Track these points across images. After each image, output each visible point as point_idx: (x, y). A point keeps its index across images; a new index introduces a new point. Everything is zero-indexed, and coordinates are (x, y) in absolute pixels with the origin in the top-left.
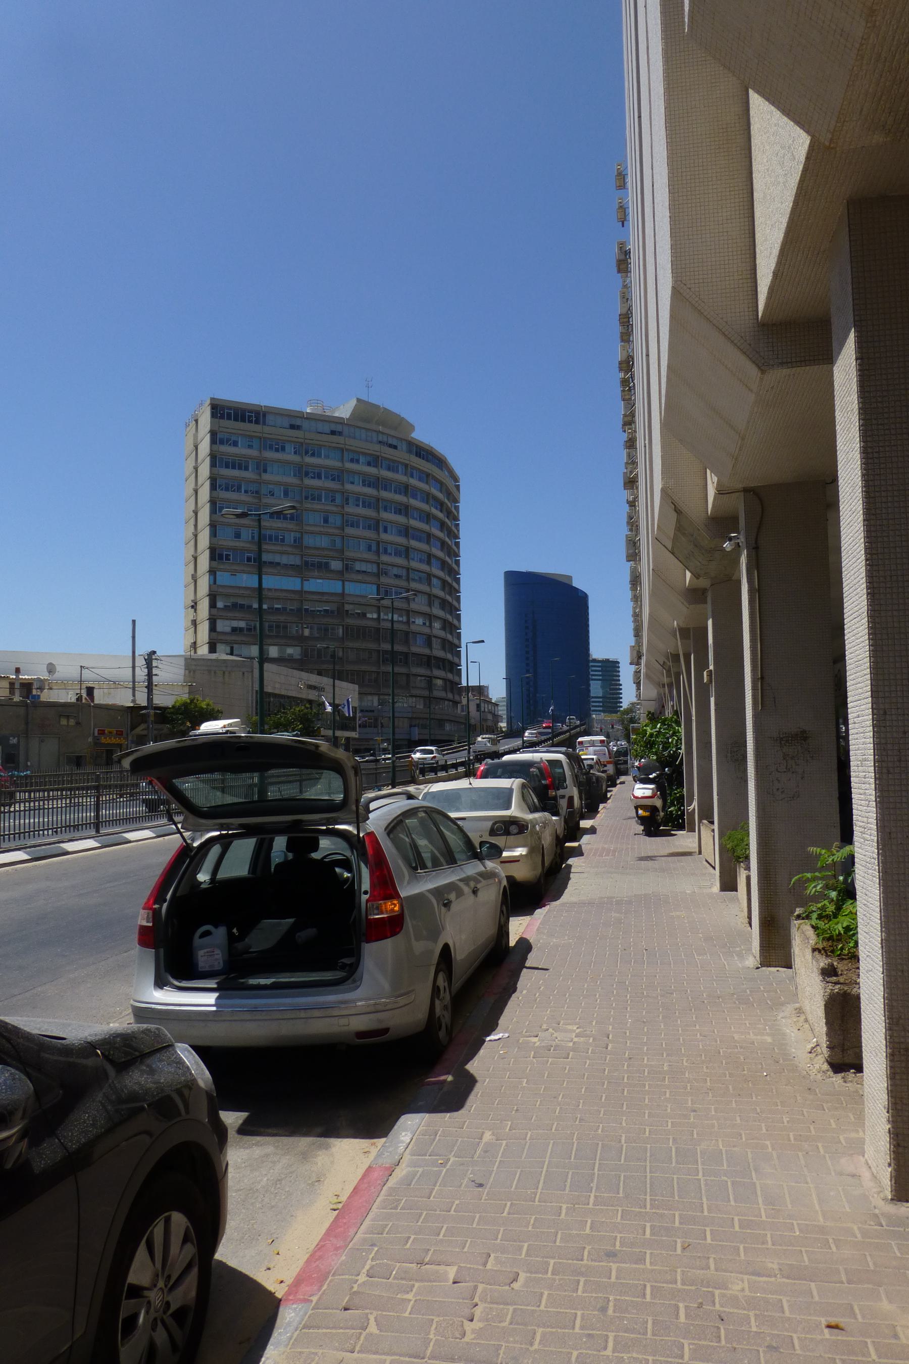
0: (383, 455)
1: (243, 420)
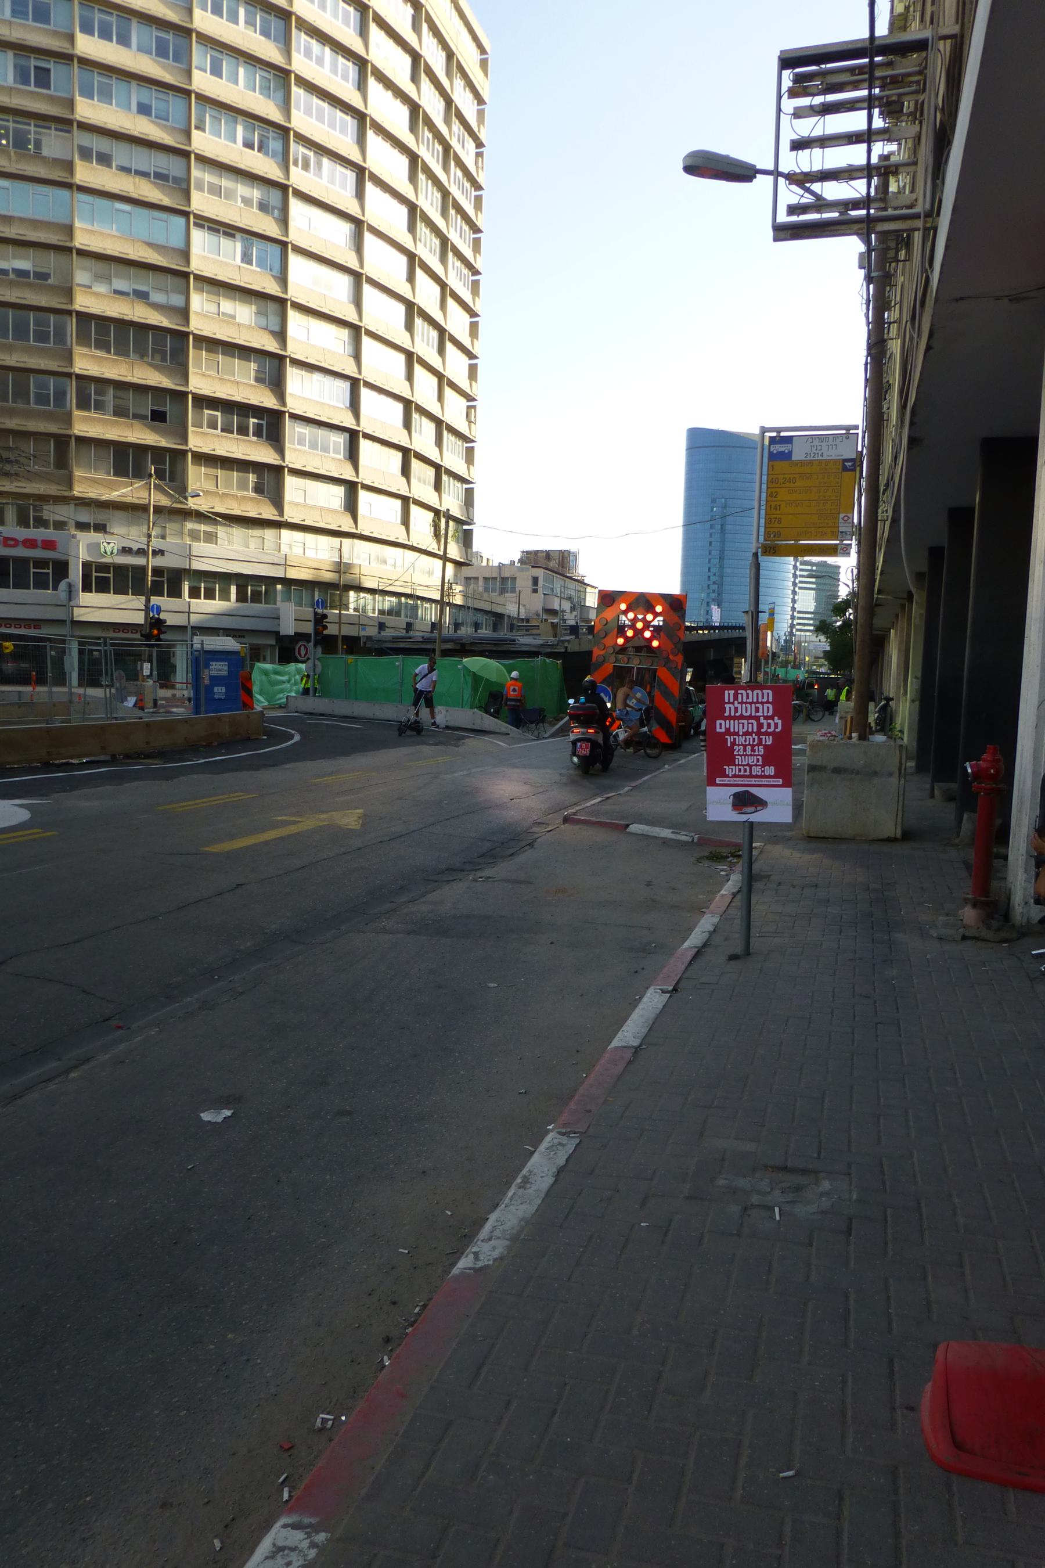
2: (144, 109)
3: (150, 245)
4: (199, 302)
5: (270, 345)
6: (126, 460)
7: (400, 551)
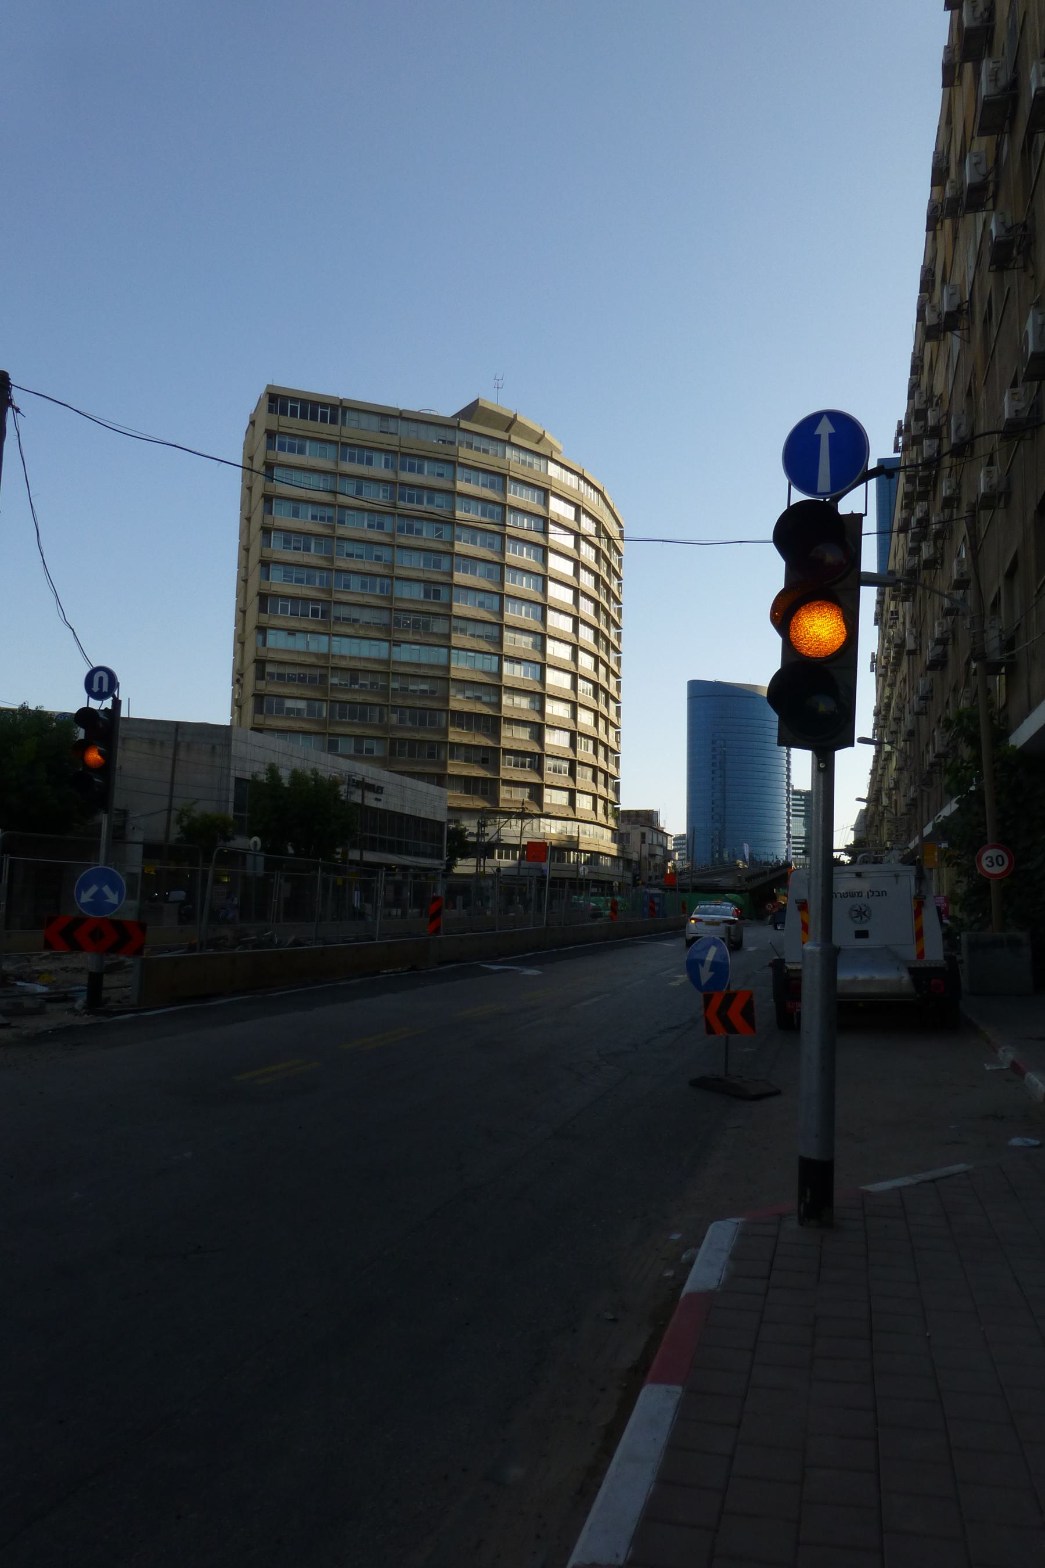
0: (511, 474)
1: (314, 418)
2: (481, 605)
3: (484, 672)
4: (506, 700)
5: (538, 719)
6: (469, 784)
7: (570, 823)
